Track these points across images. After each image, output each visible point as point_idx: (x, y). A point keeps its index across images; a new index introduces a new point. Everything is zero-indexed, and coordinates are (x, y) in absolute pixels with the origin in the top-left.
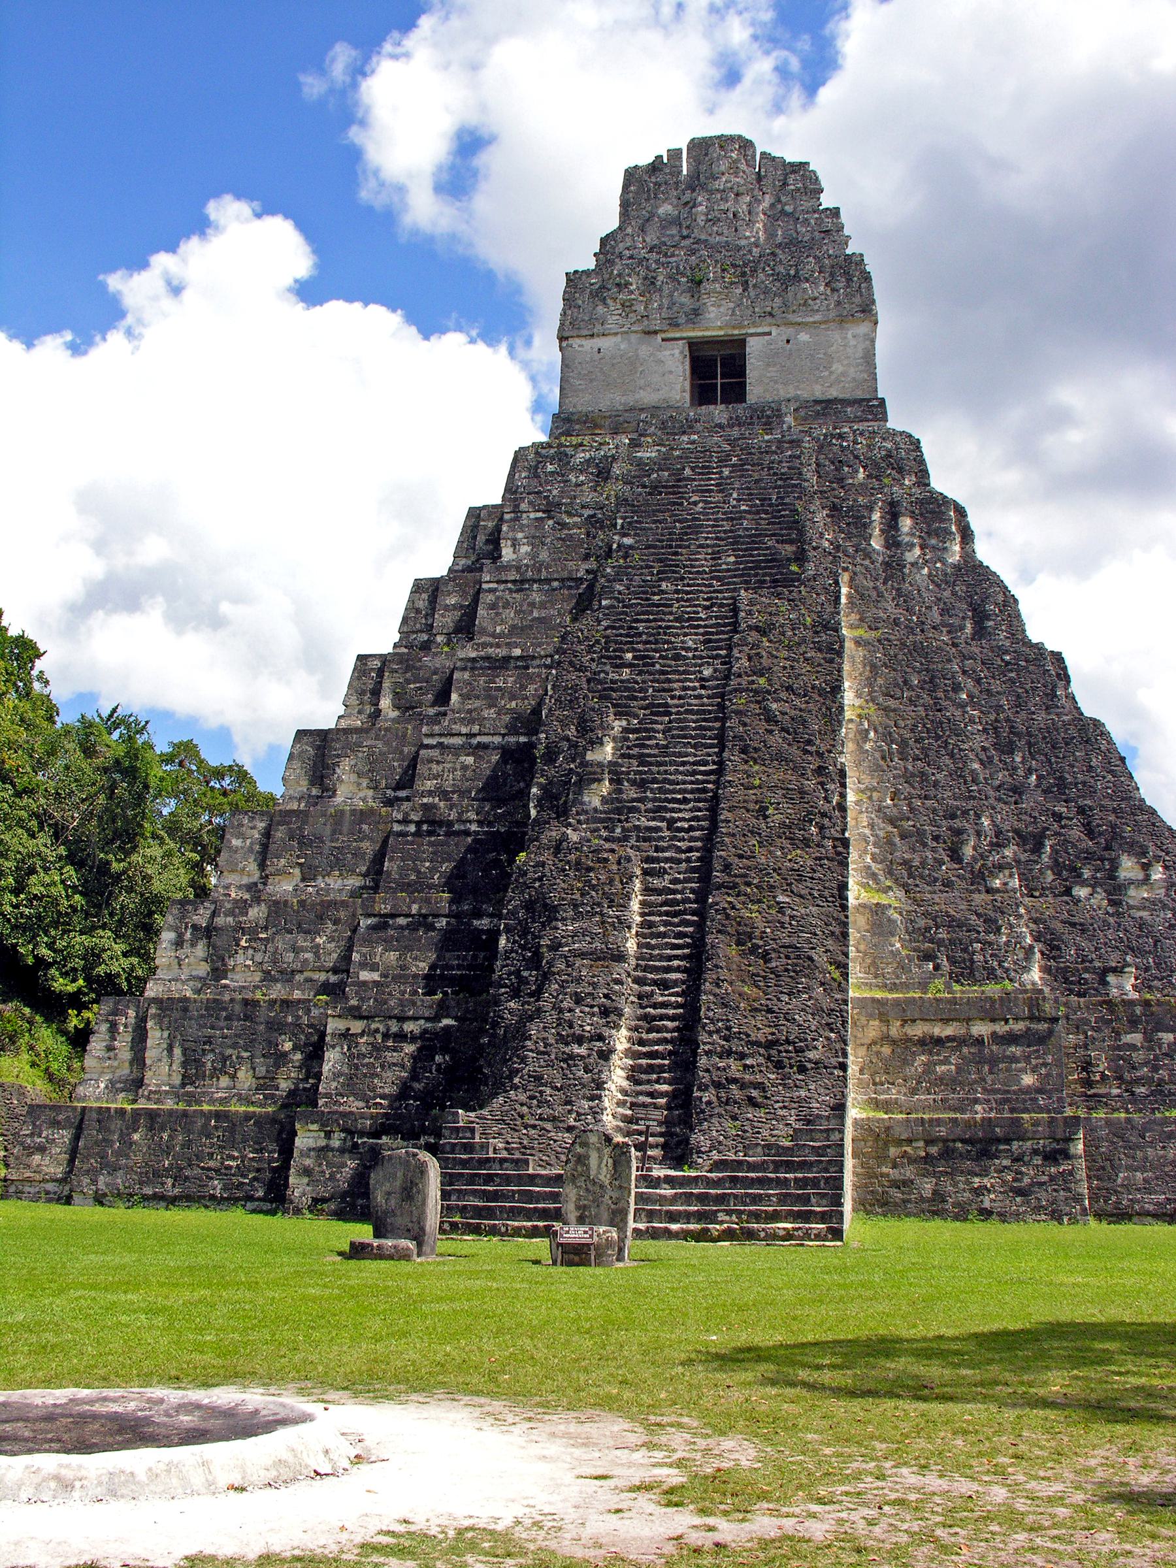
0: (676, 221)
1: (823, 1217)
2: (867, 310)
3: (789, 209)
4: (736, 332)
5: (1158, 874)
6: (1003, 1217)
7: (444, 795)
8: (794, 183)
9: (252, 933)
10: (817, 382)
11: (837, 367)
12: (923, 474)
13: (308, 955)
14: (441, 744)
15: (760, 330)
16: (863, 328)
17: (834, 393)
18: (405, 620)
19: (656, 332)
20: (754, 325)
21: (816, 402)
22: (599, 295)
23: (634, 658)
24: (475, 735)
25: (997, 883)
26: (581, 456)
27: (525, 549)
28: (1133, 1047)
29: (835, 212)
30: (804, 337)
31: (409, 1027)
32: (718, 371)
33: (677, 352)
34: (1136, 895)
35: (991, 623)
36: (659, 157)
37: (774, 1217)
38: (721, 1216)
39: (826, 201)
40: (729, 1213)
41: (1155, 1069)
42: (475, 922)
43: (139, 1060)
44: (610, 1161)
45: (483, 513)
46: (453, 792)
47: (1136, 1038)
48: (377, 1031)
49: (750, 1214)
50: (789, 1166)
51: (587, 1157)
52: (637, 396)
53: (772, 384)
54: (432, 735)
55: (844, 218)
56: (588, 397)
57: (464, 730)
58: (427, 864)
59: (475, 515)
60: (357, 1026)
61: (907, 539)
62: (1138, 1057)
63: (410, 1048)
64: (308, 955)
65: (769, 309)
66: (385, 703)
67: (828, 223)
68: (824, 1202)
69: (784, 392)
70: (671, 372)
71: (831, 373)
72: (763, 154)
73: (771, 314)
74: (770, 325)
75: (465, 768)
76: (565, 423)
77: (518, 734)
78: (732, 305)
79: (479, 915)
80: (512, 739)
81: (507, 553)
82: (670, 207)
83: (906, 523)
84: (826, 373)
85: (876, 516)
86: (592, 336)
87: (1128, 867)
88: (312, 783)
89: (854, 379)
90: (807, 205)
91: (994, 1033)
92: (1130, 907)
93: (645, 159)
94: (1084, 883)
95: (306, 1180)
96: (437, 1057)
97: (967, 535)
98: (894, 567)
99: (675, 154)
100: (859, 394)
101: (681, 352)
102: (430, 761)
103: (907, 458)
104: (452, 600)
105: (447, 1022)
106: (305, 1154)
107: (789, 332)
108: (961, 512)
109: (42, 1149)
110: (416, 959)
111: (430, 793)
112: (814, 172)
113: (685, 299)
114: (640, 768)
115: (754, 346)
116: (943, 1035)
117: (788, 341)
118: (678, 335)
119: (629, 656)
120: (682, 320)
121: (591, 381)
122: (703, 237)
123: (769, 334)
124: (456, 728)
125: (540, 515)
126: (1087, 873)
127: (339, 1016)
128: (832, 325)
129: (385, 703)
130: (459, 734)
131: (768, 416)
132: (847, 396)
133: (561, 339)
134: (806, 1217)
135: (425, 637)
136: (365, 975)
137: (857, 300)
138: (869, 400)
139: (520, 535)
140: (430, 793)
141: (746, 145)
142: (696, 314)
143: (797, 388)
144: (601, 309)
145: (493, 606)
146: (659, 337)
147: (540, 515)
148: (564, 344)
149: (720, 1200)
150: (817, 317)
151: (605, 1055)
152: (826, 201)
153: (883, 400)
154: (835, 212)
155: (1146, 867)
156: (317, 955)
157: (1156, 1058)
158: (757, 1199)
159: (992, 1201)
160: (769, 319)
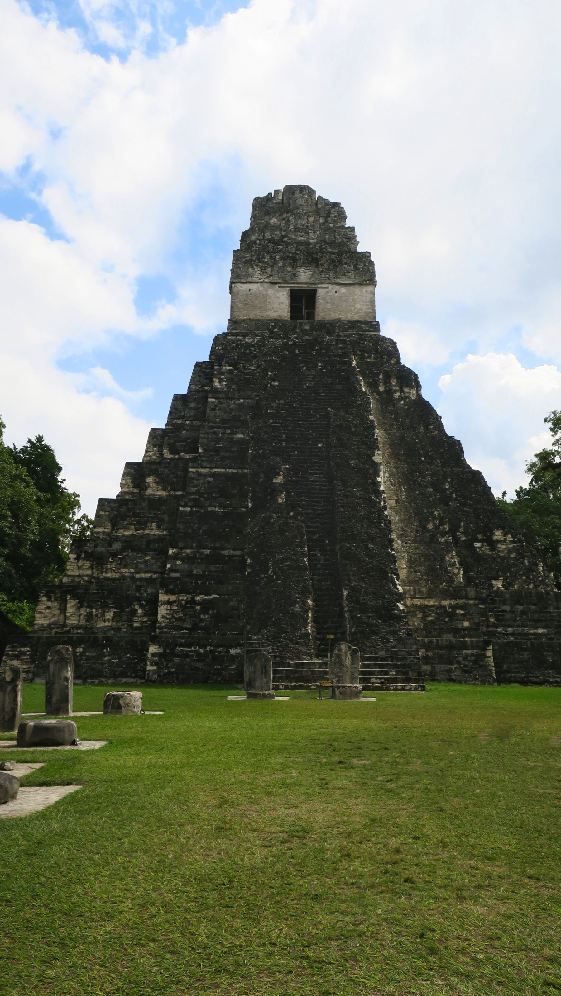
0: (278, 227)
1: (416, 681)
3: (331, 225)
4: (313, 286)
5: (509, 538)
6: (460, 682)
7: (201, 495)
8: (333, 213)
9: (114, 555)
10: (349, 312)
11: (358, 306)
12: (398, 358)
13: (142, 566)
14: (197, 472)
15: (323, 286)
16: (370, 288)
17: (356, 318)
18: (170, 413)
19: (276, 283)
20: (321, 283)
21: (349, 322)
22: (249, 263)
23: (287, 437)
24: (213, 468)
25: (443, 540)
27: (224, 383)
28: (505, 611)
29: (352, 229)
30: (343, 290)
33: (285, 293)
35: (432, 427)
36: (270, 194)
37: (395, 680)
38: (373, 680)
39: (349, 223)
40: (377, 679)
41: (515, 621)
42: (223, 552)
44: (350, 657)
45: (204, 365)
46: (205, 494)
47: (507, 608)
48: (183, 600)
49: (385, 679)
50: (398, 659)
51: (341, 655)
52: (267, 313)
53: (328, 312)
54: (193, 467)
55: (357, 232)
56: (244, 312)
57: (208, 466)
58: (196, 526)
59: (198, 365)
60: (173, 598)
61: (394, 388)
62: (508, 616)
63: (198, 608)
64: (142, 566)
65: (328, 276)
66: (165, 451)
67: (349, 234)
68: (415, 674)
69: (334, 316)
70: (283, 303)
71: (355, 308)
72: (319, 197)
73: (328, 278)
74: (328, 283)
75: (209, 482)
77: (232, 468)
78: (311, 273)
79: (224, 549)
80: (230, 470)
81: (217, 384)
82: (276, 220)
83: (394, 382)
84: (353, 308)
85: (381, 377)
86: (246, 283)
87: (498, 535)
88: (135, 487)
89: (365, 312)
90: (339, 224)
91: (450, 604)
92: (499, 551)
93: (263, 194)
94: (478, 541)
95: (155, 668)
96: (210, 612)
97: (418, 386)
99: (276, 192)
100: (367, 319)
101: (288, 294)
102: (193, 479)
103: (389, 350)
104: (192, 405)
105: (213, 596)
106: (153, 655)
107: (337, 288)
108: (416, 376)
109: (17, 657)
110: (196, 568)
111: (194, 494)
112: (343, 208)
113: (289, 269)
115: (321, 292)
116: (429, 604)
117: (336, 292)
118: (286, 285)
119: (284, 436)
120: (288, 278)
121: (247, 304)
122: (293, 237)
123: (328, 287)
124: (204, 464)
125: (231, 368)
126: (480, 537)
127: (164, 593)
128: (356, 286)
129: (165, 451)
130: (205, 468)
131: (329, 327)
132: (362, 319)
133: (232, 283)
134: (408, 680)
135: (180, 421)
136: (173, 575)
137: (368, 274)
138: (372, 322)
139: (223, 377)
140: (194, 494)
141: (312, 192)
142: (295, 275)
143: (340, 314)
144: (250, 269)
145: (214, 409)
146: (277, 286)
147: (231, 368)
148: (233, 285)
149: (371, 673)
150: (350, 282)
152: (349, 223)
153: (378, 323)
154: (352, 229)
155: (505, 535)
156: (147, 566)
157: (516, 616)
158: (386, 673)
159: (456, 675)
160: (328, 281)
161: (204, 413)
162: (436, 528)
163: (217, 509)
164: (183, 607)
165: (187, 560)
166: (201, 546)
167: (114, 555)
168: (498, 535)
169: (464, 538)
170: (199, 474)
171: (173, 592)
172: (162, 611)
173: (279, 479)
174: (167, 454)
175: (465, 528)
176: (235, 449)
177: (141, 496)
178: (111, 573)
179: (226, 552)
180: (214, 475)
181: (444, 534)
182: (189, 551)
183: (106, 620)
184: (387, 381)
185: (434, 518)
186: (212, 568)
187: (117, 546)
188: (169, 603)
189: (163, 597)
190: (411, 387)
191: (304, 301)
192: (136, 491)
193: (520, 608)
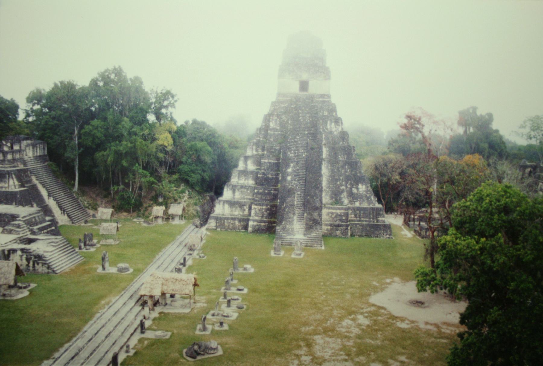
2: (329, 79)
5: (364, 187)
12: (336, 112)
17: (322, 93)
25: (342, 188)
26: (282, 105)
31: (264, 207)
32: (304, 86)
34: (360, 190)
43: (224, 209)
47: (358, 212)
60: (256, 207)
76: (279, 95)
85: (329, 122)
87: (360, 186)
97: (342, 123)
98: (331, 132)
104: (263, 133)
108: (341, 120)
114: (296, 174)
135: (258, 138)
151: (293, 220)
161: (266, 136)
162: (340, 184)
163: (270, 176)
164: (260, 210)
165: (261, 194)
166: (265, 189)
167: (238, 190)
168: (360, 186)
169: (349, 186)
170: (265, 162)
171: (256, 205)
172: (253, 212)
173: (289, 170)
174: (255, 153)
175: (351, 183)
176: (277, 152)
177: (246, 168)
178: (238, 196)
179: (272, 192)
180: (270, 163)
181: (342, 186)
182: (261, 191)
183: (237, 212)
184: (331, 124)
185: (340, 180)
186: (268, 197)
187: (239, 187)
188: (255, 209)
189: (253, 206)
190: (339, 125)
191: (304, 86)
192: (245, 166)
193: (362, 212)
